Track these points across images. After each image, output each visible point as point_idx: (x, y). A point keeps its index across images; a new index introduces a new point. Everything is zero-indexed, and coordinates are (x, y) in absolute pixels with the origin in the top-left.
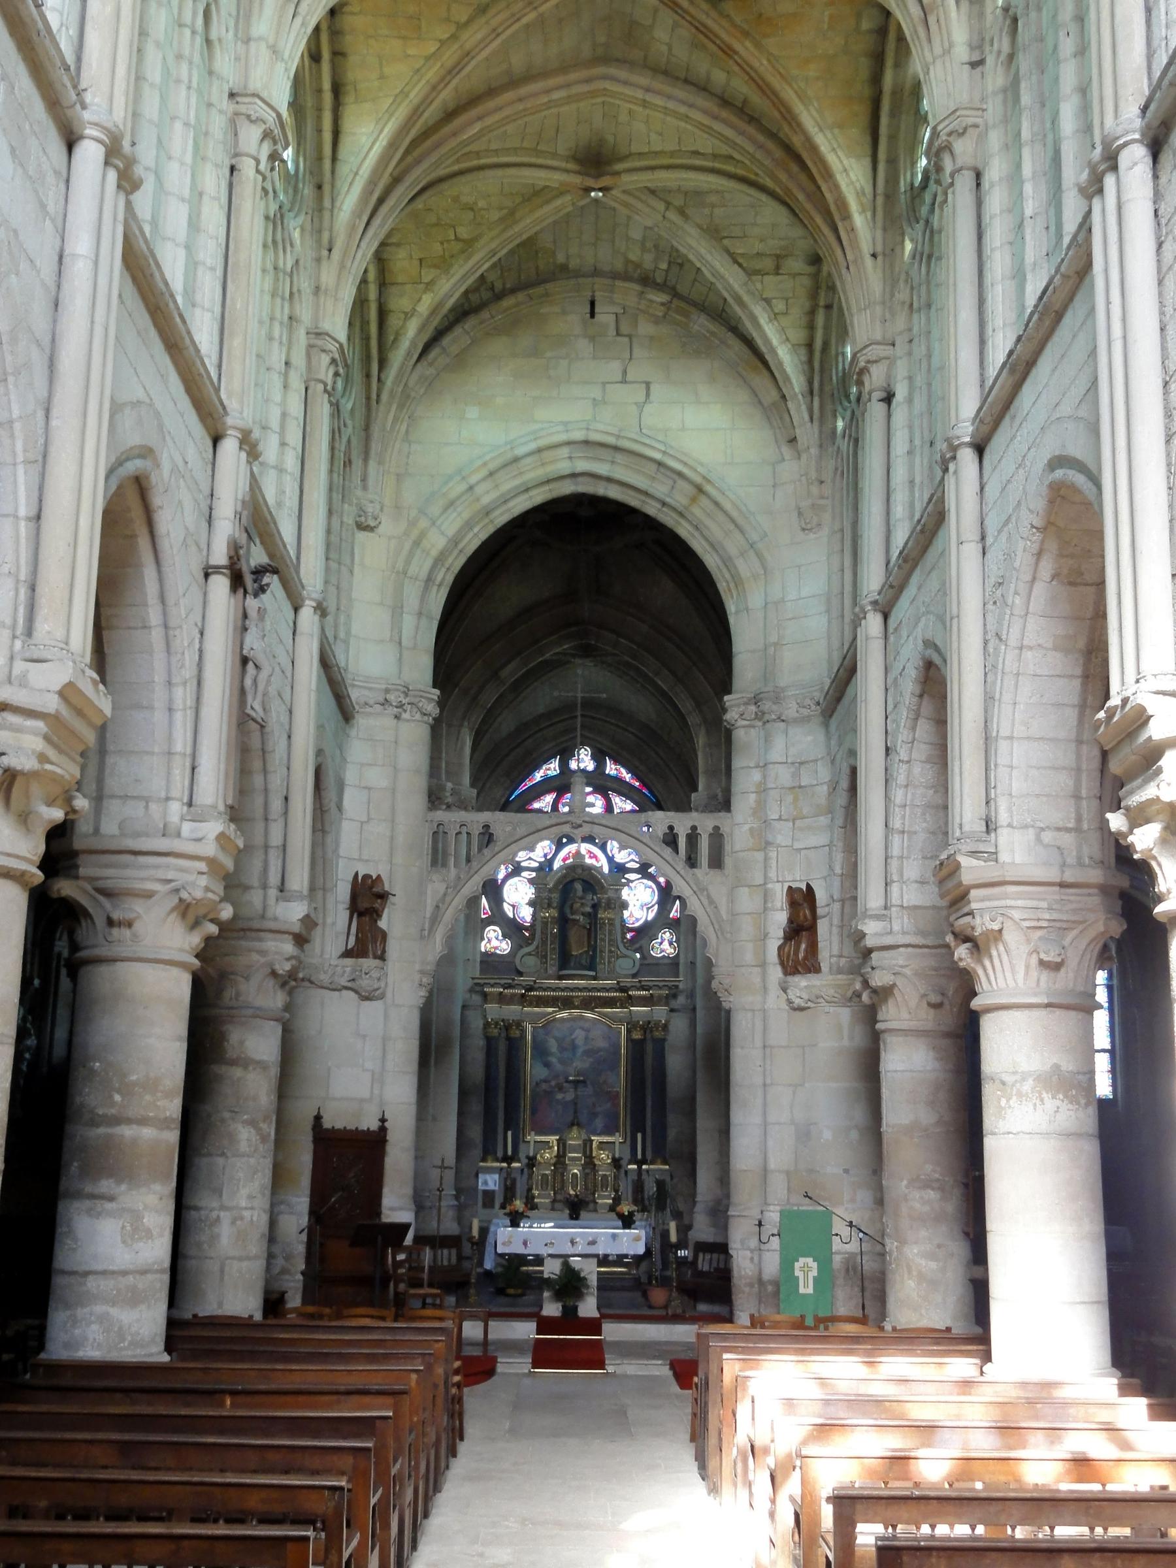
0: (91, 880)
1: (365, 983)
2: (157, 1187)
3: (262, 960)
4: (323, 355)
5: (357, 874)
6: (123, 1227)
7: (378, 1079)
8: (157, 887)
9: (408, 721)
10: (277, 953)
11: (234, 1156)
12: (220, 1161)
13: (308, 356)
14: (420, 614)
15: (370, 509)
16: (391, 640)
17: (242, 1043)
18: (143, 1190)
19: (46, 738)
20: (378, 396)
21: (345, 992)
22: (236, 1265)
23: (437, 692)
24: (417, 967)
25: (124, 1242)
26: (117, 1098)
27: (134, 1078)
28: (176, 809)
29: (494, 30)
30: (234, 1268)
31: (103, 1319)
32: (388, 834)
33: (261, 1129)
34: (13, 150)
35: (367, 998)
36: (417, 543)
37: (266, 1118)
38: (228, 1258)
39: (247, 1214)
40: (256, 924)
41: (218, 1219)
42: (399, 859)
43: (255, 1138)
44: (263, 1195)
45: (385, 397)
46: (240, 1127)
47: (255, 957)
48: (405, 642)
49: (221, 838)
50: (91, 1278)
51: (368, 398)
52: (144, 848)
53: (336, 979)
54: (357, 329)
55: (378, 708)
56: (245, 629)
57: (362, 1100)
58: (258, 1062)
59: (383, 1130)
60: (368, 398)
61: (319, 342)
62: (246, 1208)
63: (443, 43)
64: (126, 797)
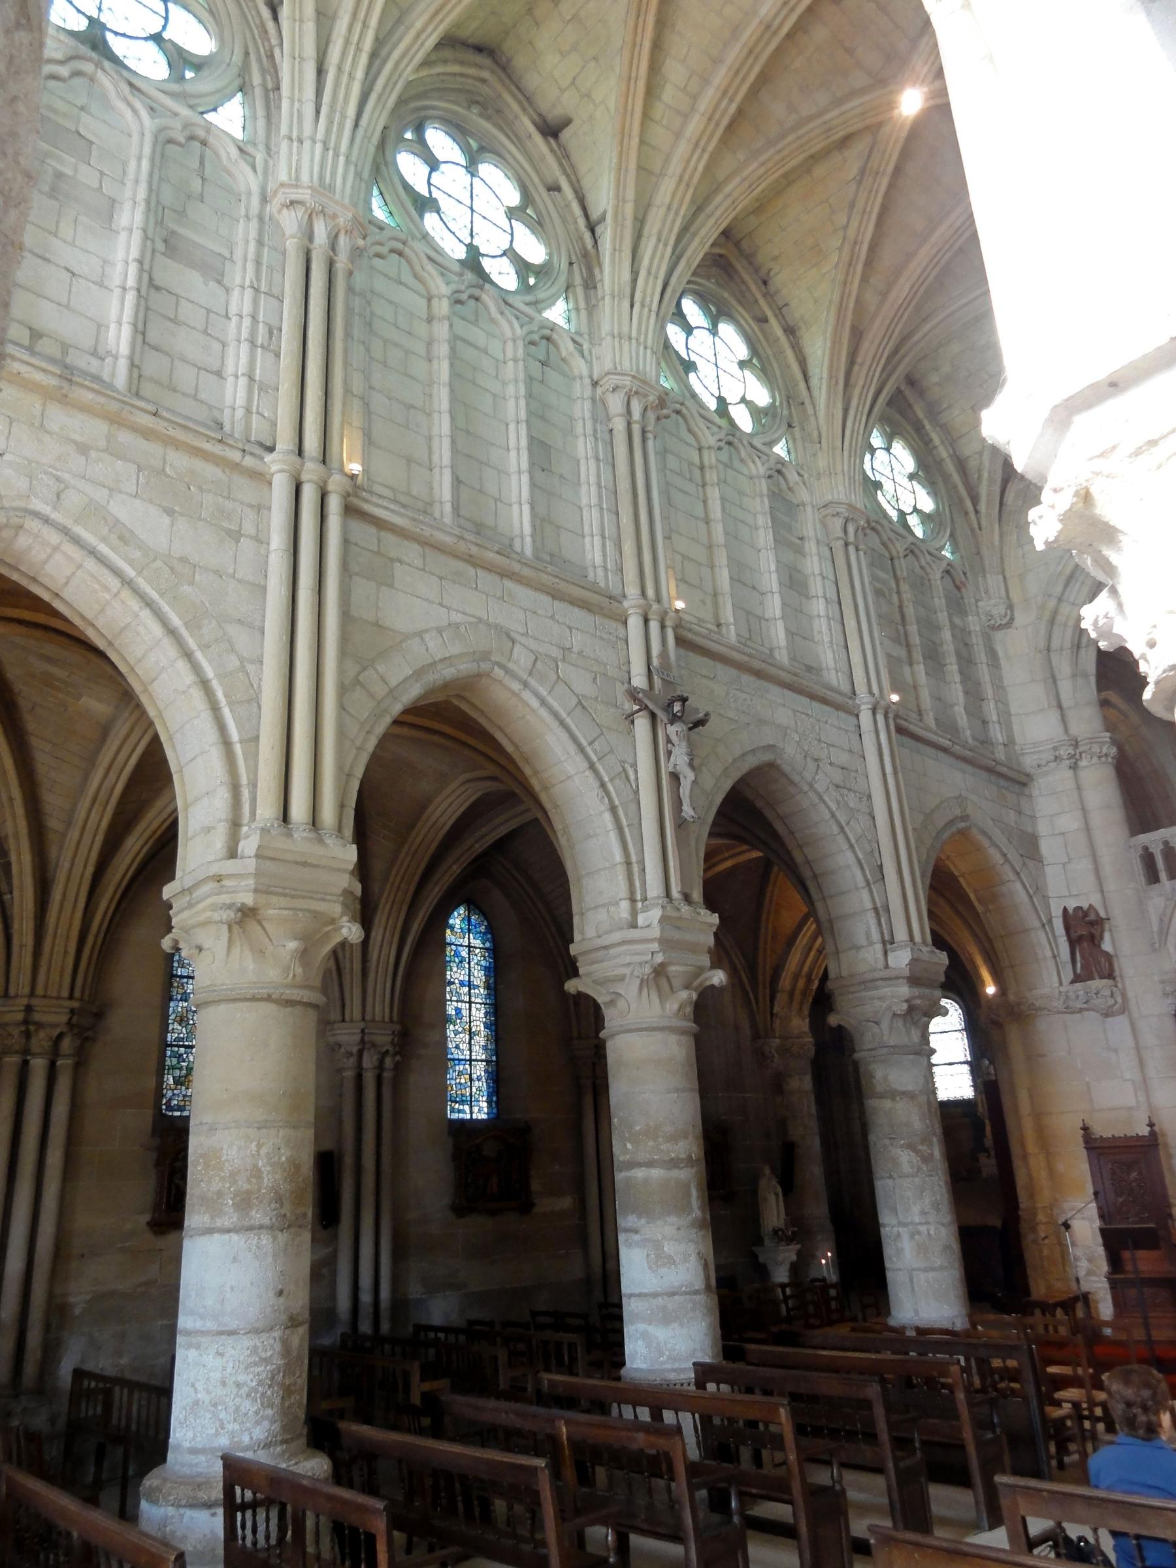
0: (588, 974)
1: (1097, 1002)
2: (673, 1219)
3: (885, 1005)
4: (835, 519)
5: (1065, 910)
6: (648, 1256)
7: (1145, 1085)
8: (627, 971)
9: (1086, 767)
10: (893, 997)
11: (900, 1177)
12: (890, 1182)
13: (824, 525)
14: (1074, 676)
15: (995, 612)
16: (1049, 707)
17: (885, 1078)
18: (659, 1222)
19: (256, 891)
20: (979, 524)
21: (1086, 1013)
22: (922, 1276)
23: (1108, 734)
24: (1156, 978)
25: (650, 1268)
26: (629, 1146)
27: (638, 1128)
28: (625, 905)
29: (864, 212)
30: (922, 1278)
31: (645, 1336)
32: (1090, 866)
33: (920, 1151)
34: (170, 512)
35: (1107, 1015)
36: (1052, 622)
37: (925, 1140)
38: (914, 1270)
39: (923, 1229)
40: (869, 976)
41: (899, 1235)
42: (1111, 886)
43: (916, 1159)
44: (938, 1210)
45: (984, 523)
46: (899, 1152)
47: (877, 1003)
48: (1065, 704)
49: (663, 920)
50: (633, 1300)
51: (973, 530)
52: (607, 943)
53: (1071, 1004)
54: (941, 484)
55: (1053, 765)
56: (669, 753)
57: (1130, 1109)
58: (904, 1093)
59: (1153, 1134)
60: (973, 530)
61: (829, 511)
62: (921, 1224)
63: (840, 249)
64: (596, 907)
